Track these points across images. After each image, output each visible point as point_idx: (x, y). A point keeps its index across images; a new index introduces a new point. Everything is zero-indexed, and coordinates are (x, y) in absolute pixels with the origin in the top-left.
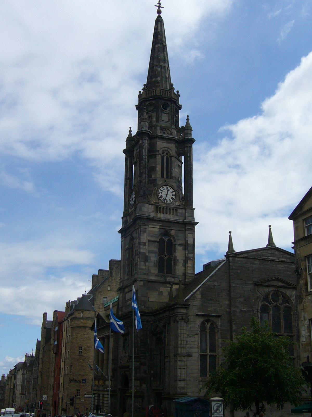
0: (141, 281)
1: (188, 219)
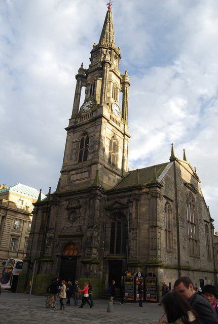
0: (101, 164)
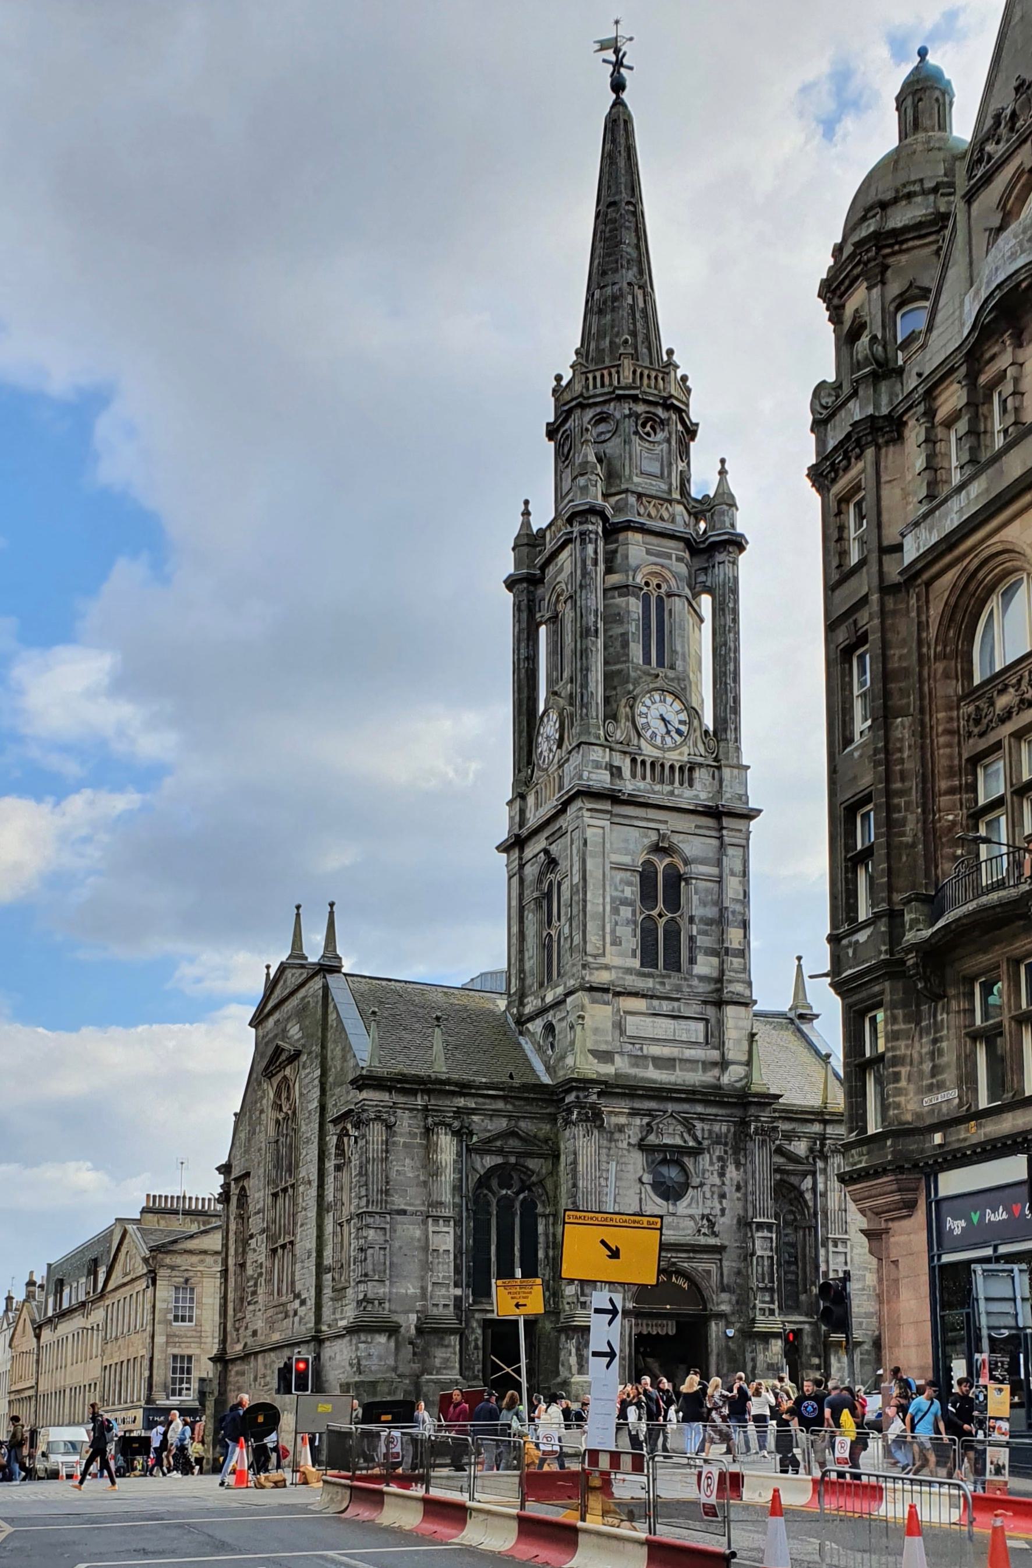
1: (727, 800)
